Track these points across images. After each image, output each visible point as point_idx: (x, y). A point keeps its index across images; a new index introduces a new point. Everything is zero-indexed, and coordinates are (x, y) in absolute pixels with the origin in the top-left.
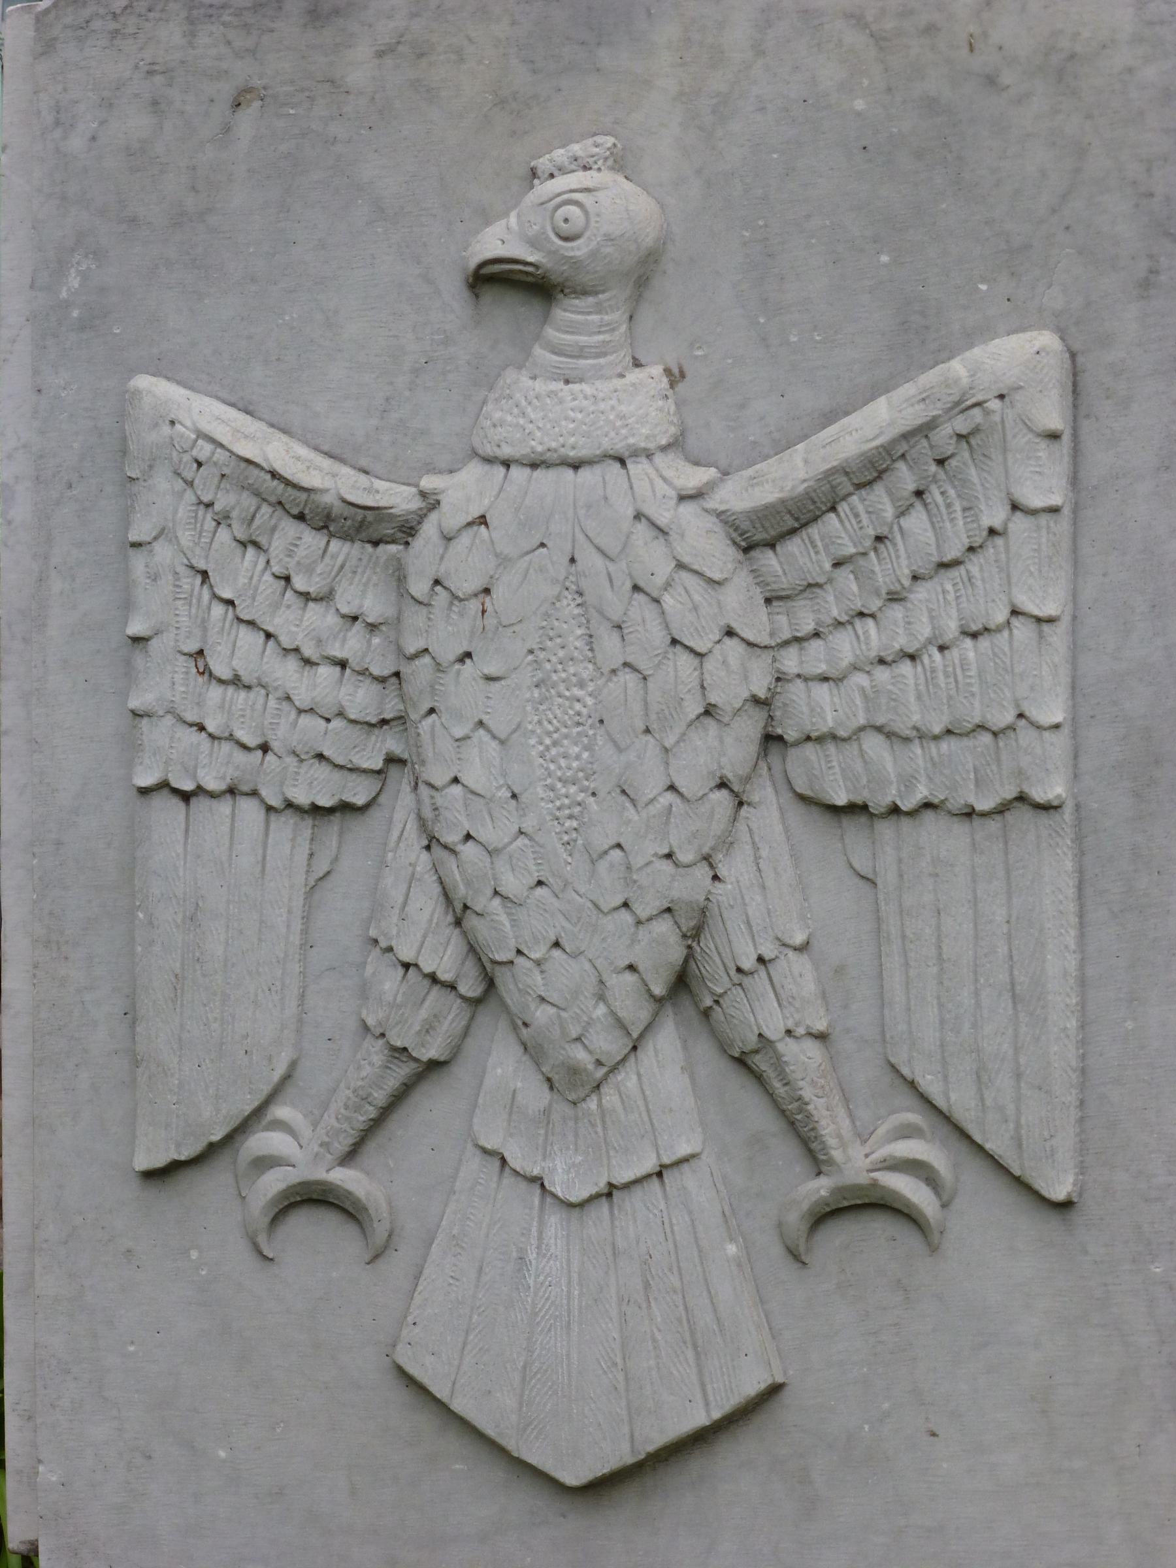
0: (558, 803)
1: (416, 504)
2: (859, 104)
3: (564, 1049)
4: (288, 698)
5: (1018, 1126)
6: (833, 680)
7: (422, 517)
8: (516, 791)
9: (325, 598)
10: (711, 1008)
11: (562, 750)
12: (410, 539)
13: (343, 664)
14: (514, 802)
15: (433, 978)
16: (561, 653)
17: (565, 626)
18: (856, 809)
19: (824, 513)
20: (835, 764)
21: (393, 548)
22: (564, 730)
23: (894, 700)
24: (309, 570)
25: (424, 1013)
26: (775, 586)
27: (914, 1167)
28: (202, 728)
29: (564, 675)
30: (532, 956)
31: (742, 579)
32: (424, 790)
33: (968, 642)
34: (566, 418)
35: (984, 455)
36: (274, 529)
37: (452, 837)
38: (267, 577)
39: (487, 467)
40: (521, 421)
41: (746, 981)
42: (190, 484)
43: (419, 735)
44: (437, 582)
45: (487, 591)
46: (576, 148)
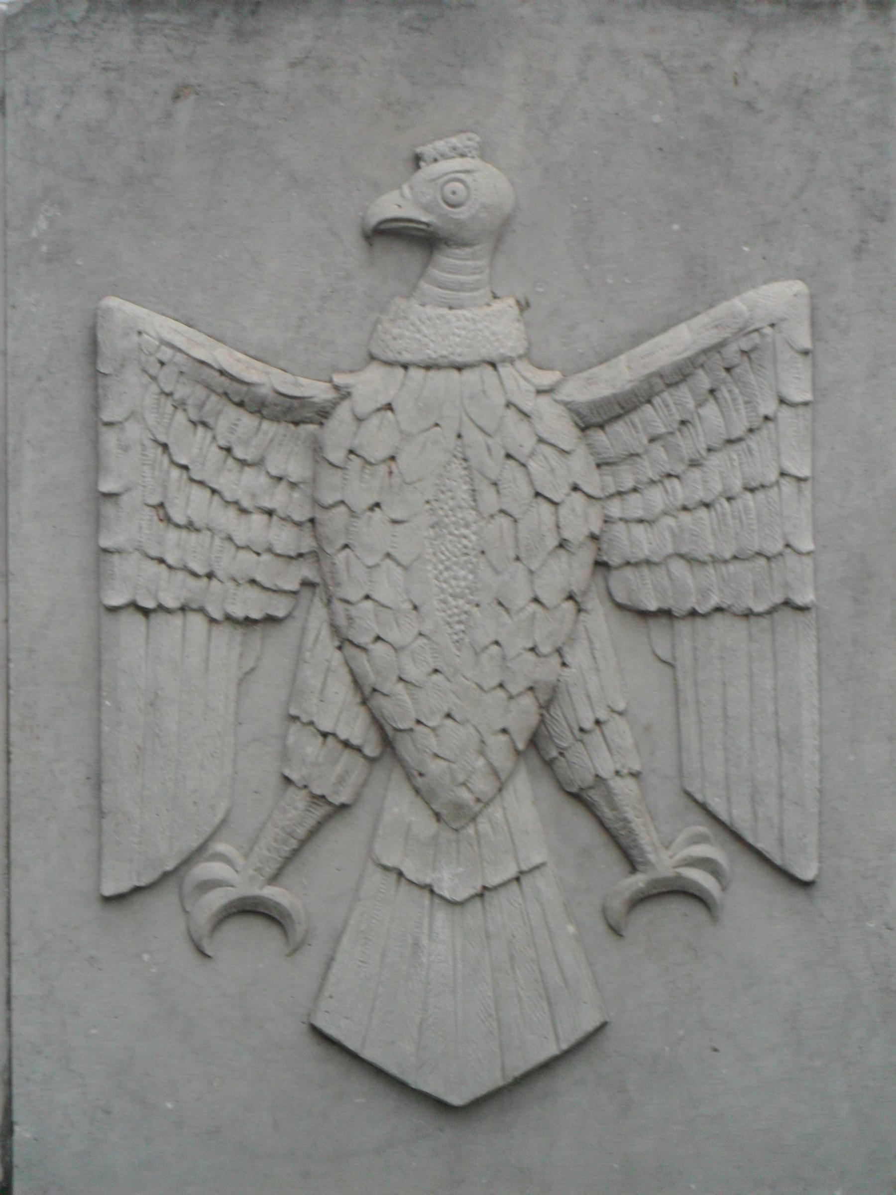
0: (449, 612)
1: (331, 395)
2: (656, 118)
3: (452, 791)
4: (230, 539)
5: (781, 830)
6: (647, 522)
7: (335, 404)
8: (417, 603)
9: (258, 464)
10: (556, 758)
11: (452, 573)
12: (323, 421)
13: (270, 513)
14: (414, 612)
15: (346, 744)
16: (451, 503)
17: (454, 483)
18: (666, 613)
19: (642, 403)
20: (648, 581)
21: (311, 427)
22: (454, 559)
23: (695, 536)
24: (246, 443)
25: (339, 769)
26: (605, 456)
27: (705, 863)
28: (161, 561)
29: (453, 519)
30: (430, 724)
31: (581, 451)
32: (339, 607)
33: (748, 495)
34: (454, 334)
35: (761, 366)
36: (219, 413)
37: (364, 639)
38: (214, 449)
39: (388, 369)
40: (418, 336)
41: (586, 737)
42: (154, 378)
43: (334, 564)
44: (351, 452)
45: (393, 458)
46: (454, 141)
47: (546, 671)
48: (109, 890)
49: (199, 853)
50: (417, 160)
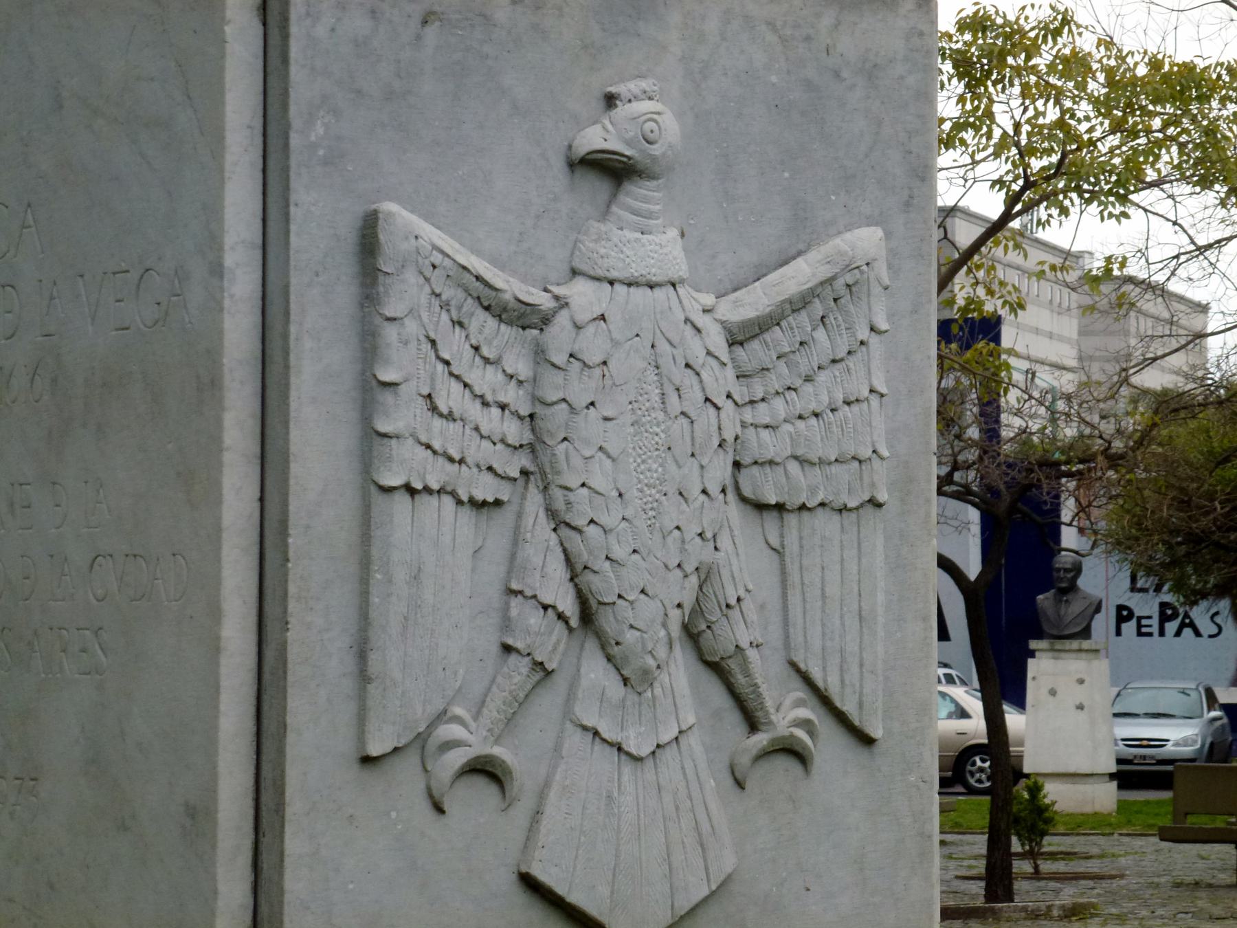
0: (645, 500)
2: (774, 79)
3: (643, 658)
4: (477, 429)
5: (861, 694)
6: (771, 427)
7: (555, 312)
8: (623, 491)
10: (704, 631)
11: (647, 466)
12: (544, 327)
13: (503, 407)
14: (619, 499)
16: (647, 404)
17: (649, 387)
18: (780, 507)
19: (774, 325)
20: (770, 479)
21: (535, 332)
22: (649, 454)
23: (809, 440)
24: (490, 343)
25: (554, 638)
26: (744, 369)
28: (428, 447)
29: (649, 418)
30: (630, 598)
33: (846, 408)
34: (649, 256)
35: (858, 298)
36: (472, 314)
37: (581, 522)
38: (467, 347)
39: (597, 284)
40: (622, 256)
41: (730, 612)
42: (427, 280)
43: (554, 455)
44: (571, 355)
45: (605, 363)
46: (644, 84)
47: (699, 553)
48: (374, 750)
49: (442, 716)
50: (610, 100)
